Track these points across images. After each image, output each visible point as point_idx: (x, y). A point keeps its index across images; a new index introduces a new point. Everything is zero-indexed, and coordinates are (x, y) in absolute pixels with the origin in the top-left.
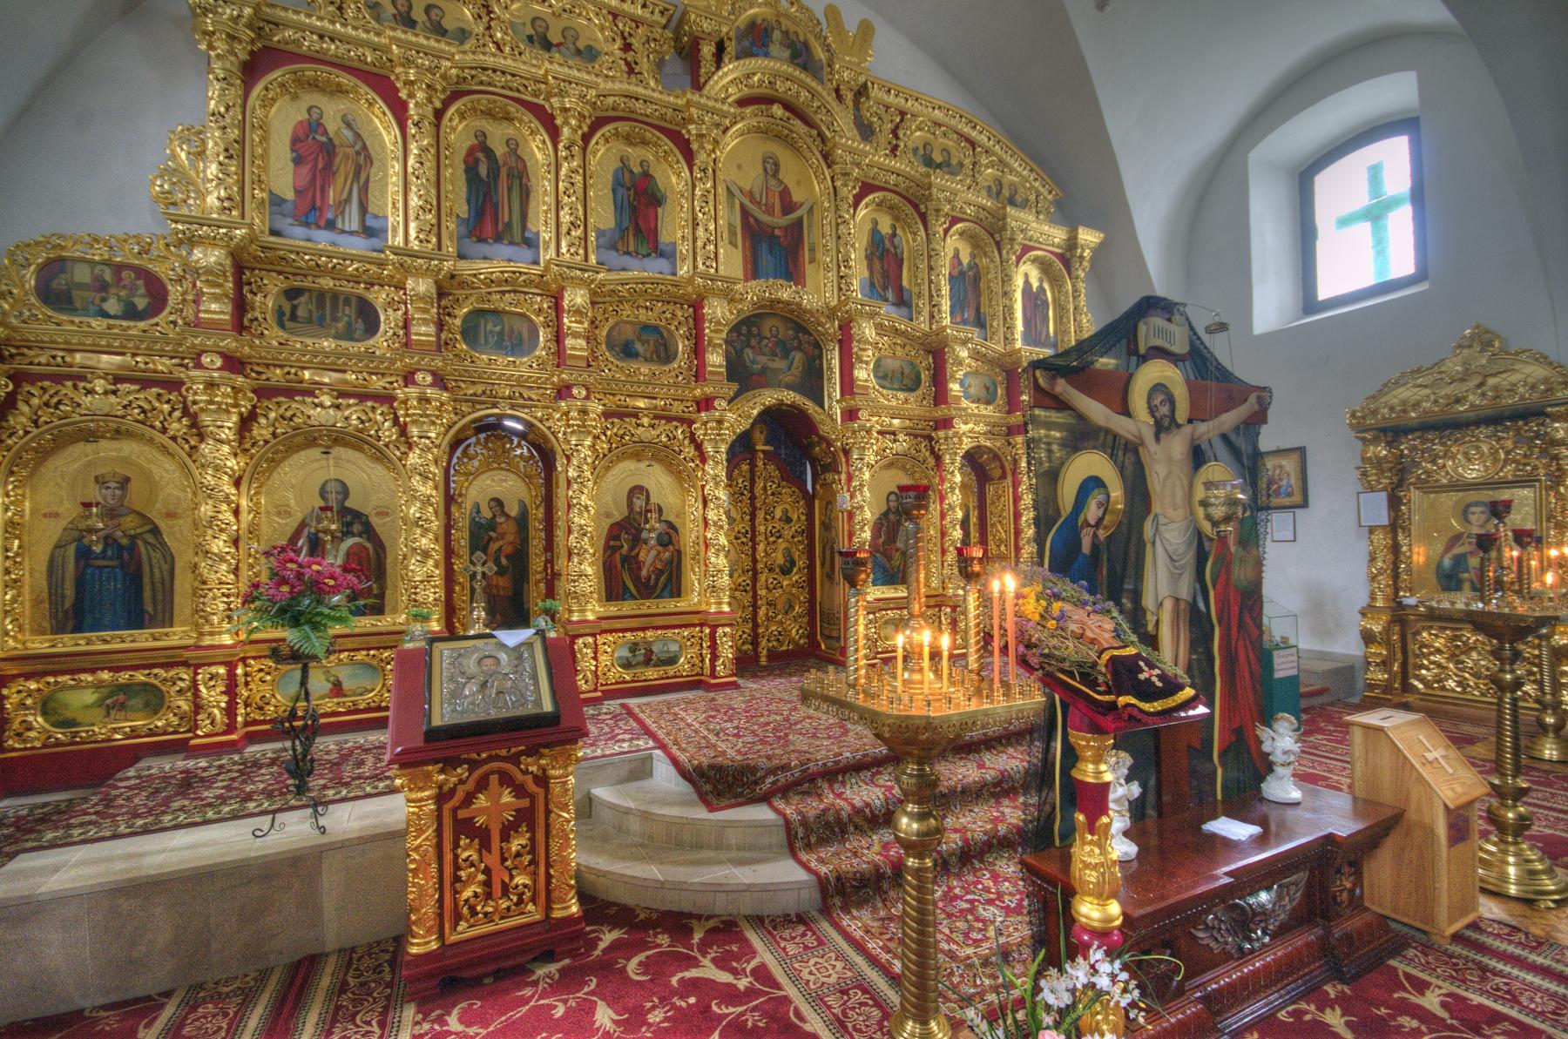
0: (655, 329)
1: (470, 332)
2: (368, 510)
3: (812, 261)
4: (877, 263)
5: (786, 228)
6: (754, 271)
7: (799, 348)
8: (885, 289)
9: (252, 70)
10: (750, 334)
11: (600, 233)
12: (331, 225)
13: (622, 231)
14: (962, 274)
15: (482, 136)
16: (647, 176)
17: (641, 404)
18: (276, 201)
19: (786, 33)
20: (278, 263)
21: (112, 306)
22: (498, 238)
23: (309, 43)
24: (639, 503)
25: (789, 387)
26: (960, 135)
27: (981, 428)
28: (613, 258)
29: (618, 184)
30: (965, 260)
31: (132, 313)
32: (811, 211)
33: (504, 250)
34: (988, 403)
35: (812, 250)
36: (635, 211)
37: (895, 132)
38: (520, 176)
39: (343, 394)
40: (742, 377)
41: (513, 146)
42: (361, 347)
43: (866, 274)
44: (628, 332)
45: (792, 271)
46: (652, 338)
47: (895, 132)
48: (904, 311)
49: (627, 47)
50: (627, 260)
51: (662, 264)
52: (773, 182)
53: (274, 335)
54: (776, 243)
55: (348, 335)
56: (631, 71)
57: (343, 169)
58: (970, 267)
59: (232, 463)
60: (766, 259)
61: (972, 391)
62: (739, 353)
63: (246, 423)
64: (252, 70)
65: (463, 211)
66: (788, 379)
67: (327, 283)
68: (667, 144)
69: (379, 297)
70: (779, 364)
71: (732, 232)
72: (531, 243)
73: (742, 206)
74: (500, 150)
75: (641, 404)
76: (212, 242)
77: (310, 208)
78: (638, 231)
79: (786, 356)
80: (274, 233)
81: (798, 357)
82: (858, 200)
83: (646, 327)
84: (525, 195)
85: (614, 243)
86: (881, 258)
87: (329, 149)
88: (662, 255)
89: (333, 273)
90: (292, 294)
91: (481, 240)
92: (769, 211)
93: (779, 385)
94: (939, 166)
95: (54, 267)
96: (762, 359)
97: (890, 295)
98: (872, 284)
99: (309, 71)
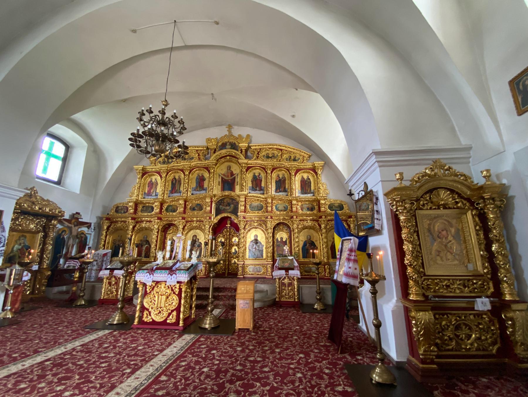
0: (200, 205)
1: (167, 210)
2: (150, 240)
3: (237, 185)
4: (254, 182)
5: (231, 180)
6: (223, 189)
7: (233, 204)
8: (256, 187)
9: (143, 175)
10: (221, 202)
11: (193, 188)
12: (151, 195)
13: (197, 187)
14: (280, 180)
15: (174, 177)
16: (203, 176)
17: (195, 219)
18: (145, 193)
19: (230, 143)
20: (141, 203)
21: (122, 212)
22: (175, 193)
23: (150, 170)
24: (194, 238)
25: (229, 212)
26: (277, 149)
27: (281, 218)
28: (195, 192)
29: (197, 178)
30: (281, 176)
31: (124, 213)
32: (238, 175)
33: (176, 194)
34: (285, 211)
35: (237, 183)
36: (199, 183)
37: (258, 154)
38: (180, 181)
39: (147, 222)
40: (218, 212)
41: (179, 177)
42: (150, 214)
43: (251, 185)
44: (194, 205)
45: (232, 189)
46: (199, 206)
47: (258, 154)
48: (262, 192)
49: (199, 155)
50: (197, 192)
51: (204, 192)
52: (229, 171)
53: (140, 213)
54: (228, 183)
55: (150, 212)
56: (199, 159)
57: (154, 186)
58: (282, 178)
59: (131, 233)
60: (226, 185)
61: (280, 208)
62: (219, 207)
63: (134, 227)
64: (143, 175)
65: (170, 189)
66: (229, 211)
67: (147, 205)
68: (206, 170)
69: (154, 206)
70: (228, 208)
71: (219, 182)
72: (180, 192)
73: (222, 177)
74: (177, 178)
75: (195, 219)
76: (132, 202)
77: (149, 194)
78: (200, 187)
79: (229, 206)
80: (144, 198)
81: (232, 206)
82: (247, 170)
83: (198, 204)
84: (180, 184)
85: (195, 189)
86: (256, 181)
87: (153, 184)
88: (204, 190)
89: (149, 203)
90: (143, 207)
91: (173, 193)
92: (228, 176)
93: (227, 212)
94: (271, 158)
95: (117, 207)
96: (224, 207)
97: (258, 189)
98: (253, 187)
99: (150, 174)
